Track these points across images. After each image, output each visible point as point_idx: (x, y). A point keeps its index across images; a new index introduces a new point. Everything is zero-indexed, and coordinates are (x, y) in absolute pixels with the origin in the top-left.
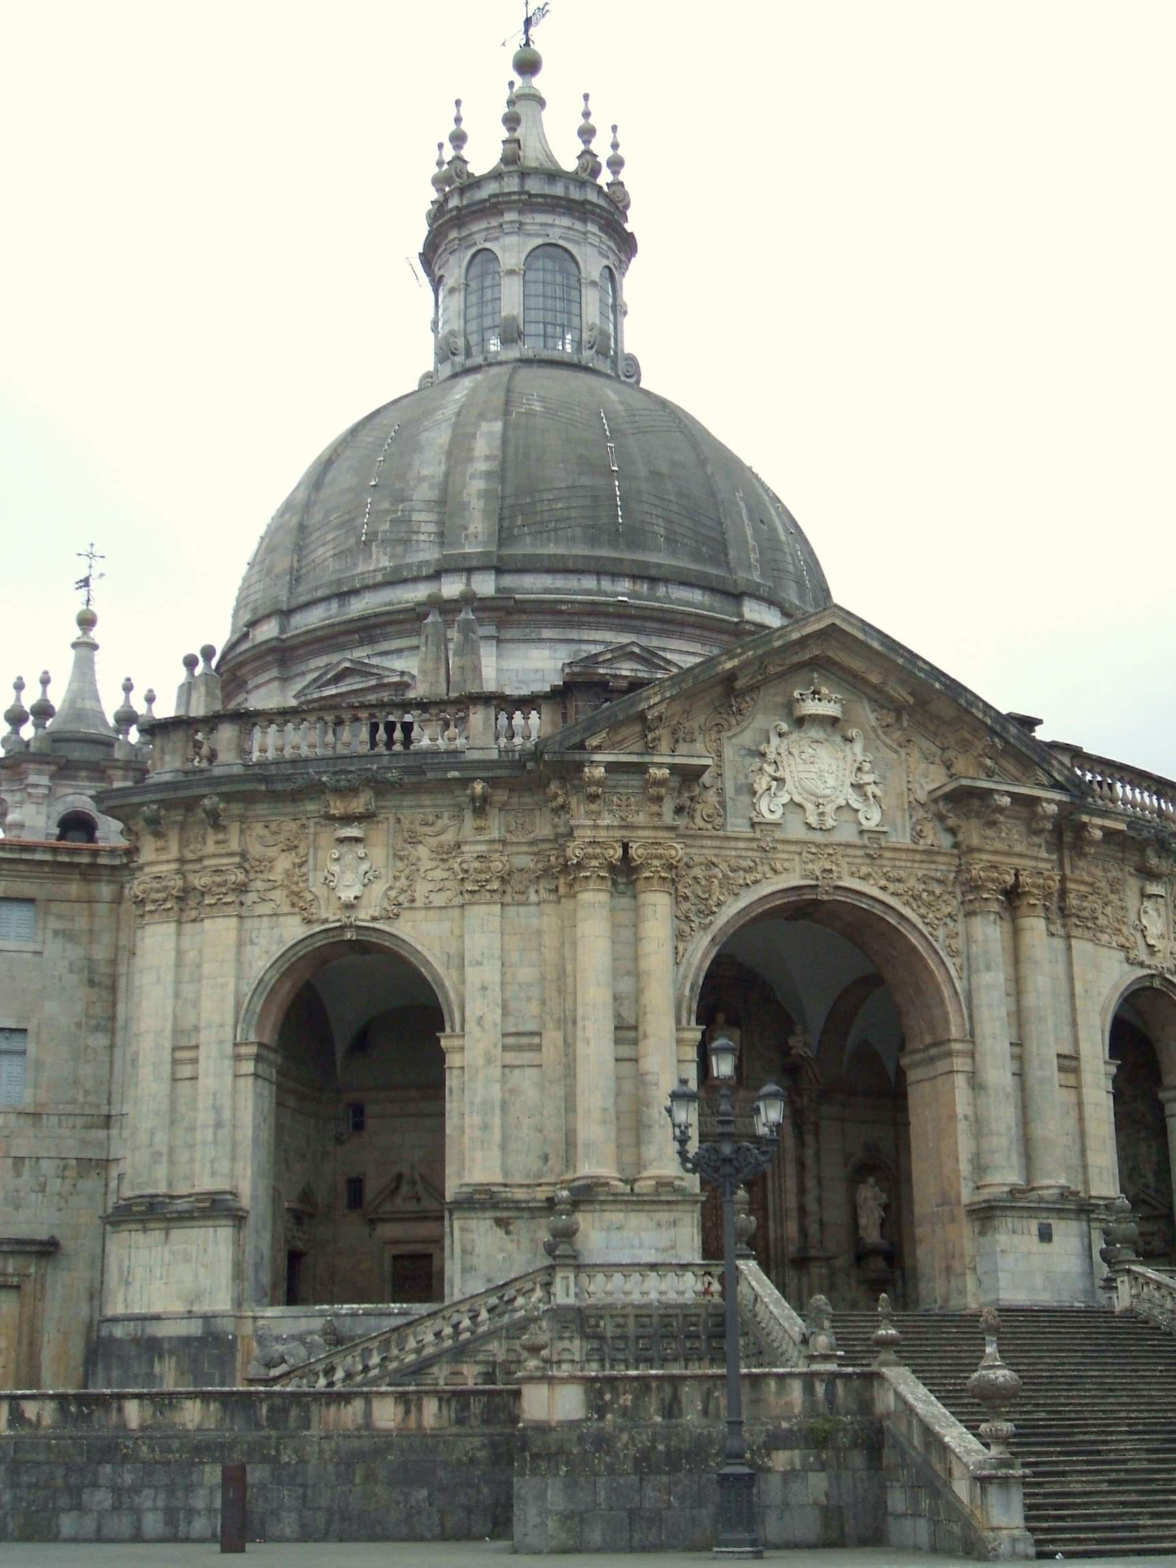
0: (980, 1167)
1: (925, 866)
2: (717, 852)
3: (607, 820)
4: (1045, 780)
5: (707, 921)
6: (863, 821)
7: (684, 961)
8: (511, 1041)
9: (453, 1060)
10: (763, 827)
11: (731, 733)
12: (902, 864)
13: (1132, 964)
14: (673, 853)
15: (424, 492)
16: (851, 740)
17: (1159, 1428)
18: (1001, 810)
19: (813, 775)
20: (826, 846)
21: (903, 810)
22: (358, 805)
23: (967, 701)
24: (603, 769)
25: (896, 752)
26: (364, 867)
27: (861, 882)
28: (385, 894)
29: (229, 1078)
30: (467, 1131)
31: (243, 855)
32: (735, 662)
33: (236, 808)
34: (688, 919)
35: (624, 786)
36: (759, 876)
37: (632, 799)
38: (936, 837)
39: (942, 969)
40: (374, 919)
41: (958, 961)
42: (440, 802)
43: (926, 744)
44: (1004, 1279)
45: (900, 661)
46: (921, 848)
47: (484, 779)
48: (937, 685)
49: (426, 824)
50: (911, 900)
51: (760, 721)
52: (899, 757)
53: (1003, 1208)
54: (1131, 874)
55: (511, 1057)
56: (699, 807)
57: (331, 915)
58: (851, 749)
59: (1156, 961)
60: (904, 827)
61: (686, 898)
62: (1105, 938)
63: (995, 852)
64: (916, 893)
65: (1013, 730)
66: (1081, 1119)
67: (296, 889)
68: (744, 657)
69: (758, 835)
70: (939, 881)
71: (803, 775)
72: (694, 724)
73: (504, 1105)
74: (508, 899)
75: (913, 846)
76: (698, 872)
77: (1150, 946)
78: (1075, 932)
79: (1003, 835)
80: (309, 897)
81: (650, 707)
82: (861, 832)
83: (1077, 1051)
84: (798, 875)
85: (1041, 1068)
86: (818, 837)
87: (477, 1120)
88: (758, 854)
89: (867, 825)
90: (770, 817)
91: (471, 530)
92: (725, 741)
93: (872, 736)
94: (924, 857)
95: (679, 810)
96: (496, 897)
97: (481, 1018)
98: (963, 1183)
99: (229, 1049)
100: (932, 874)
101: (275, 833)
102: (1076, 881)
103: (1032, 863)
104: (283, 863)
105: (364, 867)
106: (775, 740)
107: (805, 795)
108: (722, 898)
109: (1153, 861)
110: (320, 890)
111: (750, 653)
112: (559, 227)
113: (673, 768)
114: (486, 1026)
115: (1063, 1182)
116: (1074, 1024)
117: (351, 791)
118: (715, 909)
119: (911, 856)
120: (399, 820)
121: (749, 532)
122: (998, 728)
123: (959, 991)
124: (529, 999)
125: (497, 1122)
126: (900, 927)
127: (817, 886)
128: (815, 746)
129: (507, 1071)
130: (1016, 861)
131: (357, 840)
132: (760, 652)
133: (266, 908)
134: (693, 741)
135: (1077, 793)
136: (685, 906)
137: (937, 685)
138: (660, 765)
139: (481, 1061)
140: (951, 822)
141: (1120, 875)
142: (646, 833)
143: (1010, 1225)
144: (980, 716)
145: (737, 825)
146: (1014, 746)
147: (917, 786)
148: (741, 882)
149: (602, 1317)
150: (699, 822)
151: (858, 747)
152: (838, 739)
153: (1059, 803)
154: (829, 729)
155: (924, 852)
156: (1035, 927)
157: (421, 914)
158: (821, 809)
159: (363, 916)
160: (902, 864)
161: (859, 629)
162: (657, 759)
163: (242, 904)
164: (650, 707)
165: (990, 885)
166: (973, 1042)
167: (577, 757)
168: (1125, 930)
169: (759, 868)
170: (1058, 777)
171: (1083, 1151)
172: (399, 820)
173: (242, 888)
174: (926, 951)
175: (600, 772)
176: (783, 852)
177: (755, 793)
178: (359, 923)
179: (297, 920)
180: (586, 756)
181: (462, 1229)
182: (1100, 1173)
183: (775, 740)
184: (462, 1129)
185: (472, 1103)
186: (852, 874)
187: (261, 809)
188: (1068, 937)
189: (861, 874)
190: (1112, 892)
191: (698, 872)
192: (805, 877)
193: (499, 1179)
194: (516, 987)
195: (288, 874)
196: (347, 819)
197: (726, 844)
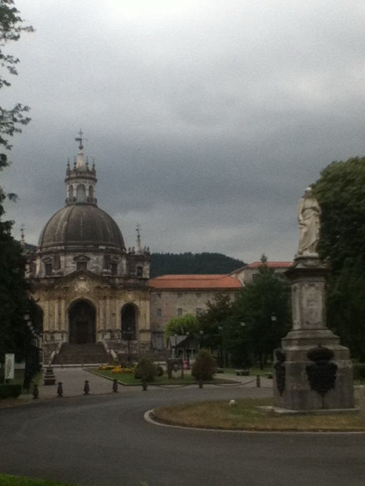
112: (81, 181)
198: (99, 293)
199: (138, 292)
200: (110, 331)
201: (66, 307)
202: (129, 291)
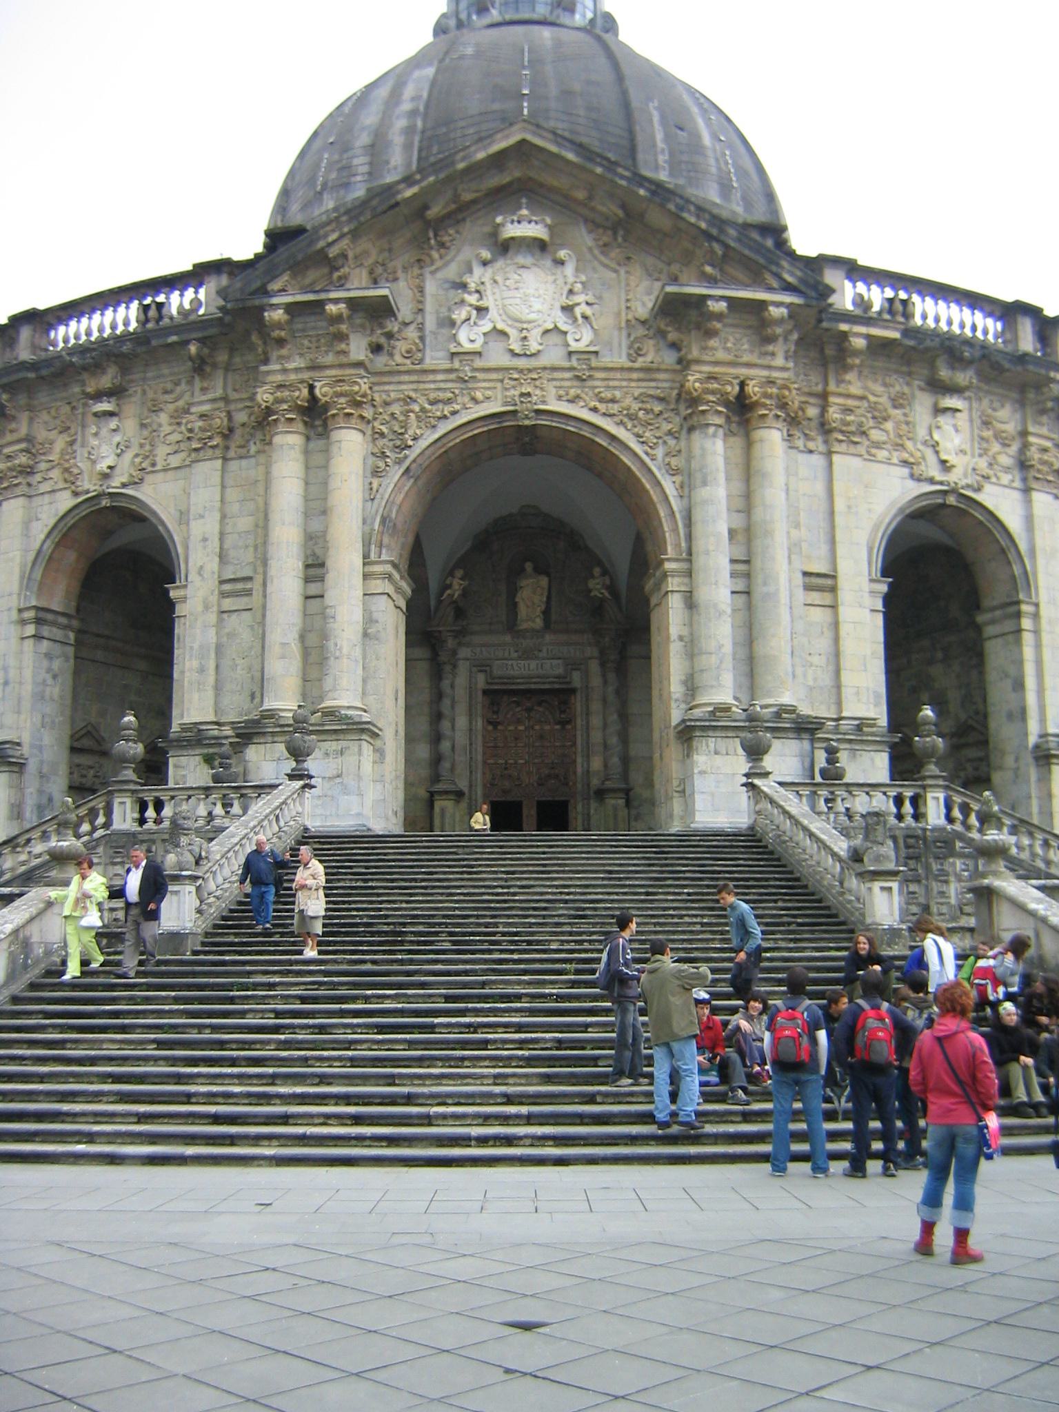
0: (692, 687)
1: (641, 384)
2: (414, 386)
3: (298, 362)
4: (775, 284)
5: (401, 456)
6: (572, 343)
7: (378, 496)
8: (227, 587)
9: (180, 610)
10: (462, 357)
11: (433, 268)
12: (616, 383)
13: (919, 480)
14: (356, 388)
15: (364, 139)
16: (562, 263)
17: (395, 967)
18: (719, 316)
19: (518, 301)
20: (530, 371)
21: (620, 329)
22: (106, 381)
23: (677, 206)
24: (281, 311)
25: (616, 271)
26: (117, 439)
27: (570, 405)
28: (133, 463)
29: (14, 641)
30: (187, 674)
31: (29, 439)
32: (415, 189)
33: (22, 399)
34: (384, 455)
35: (314, 328)
36: (457, 407)
37: (323, 340)
38: (652, 354)
39: (658, 489)
40: (124, 485)
41: (678, 479)
42: (176, 370)
43: (650, 261)
44: (700, 802)
45: (599, 170)
46: (637, 365)
47: (198, 340)
48: (642, 192)
49: (166, 392)
50: (625, 420)
51: (467, 253)
52: (619, 275)
53: (703, 728)
54: (921, 389)
55: (228, 604)
56: (397, 343)
57: (90, 485)
58: (562, 272)
59: (954, 477)
60: (620, 345)
61: (382, 435)
62: (882, 454)
63: (717, 363)
64: (632, 411)
65: (732, 232)
66: (836, 639)
67: (67, 465)
68: (424, 184)
69: (457, 365)
70: (661, 400)
71: (507, 302)
72: (398, 263)
73: (219, 649)
74: (231, 454)
75: (630, 364)
76: (396, 409)
77: (944, 462)
78: (837, 447)
79: (729, 345)
80: (76, 471)
81: (330, 245)
82: (570, 353)
83: (835, 570)
84: (500, 403)
85: (765, 584)
86: (522, 363)
87: (195, 664)
88: (458, 385)
89: (574, 346)
90: (467, 346)
91: (393, 163)
92: (428, 276)
93: (588, 256)
94: (641, 375)
95: (376, 349)
96: (218, 452)
97: (201, 567)
98: (673, 705)
99: (14, 615)
100: (651, 392)
101: (55, 418)
102: (840, 395)
103: (765, 373)
104: (60, 443)
105: (117, 439)
106: (478, 270)
107: (510, 323)
108: (418, 432)
109: (944, 373)
110: (83, 465)
111: (432, 179)
113: (352, 303)
114: (205, 576)
115: (786, 699)
116: (832, 542)
117: (96, 368)
118: (410, 443)
119: (626, 375)
120: (144, 392)
121: (659, 136)
122: (714, 232)
123: (675, 508)
124: (247, 547)
125: (212, 665)
126: (610, 448)
127: (515, 412)
128: (521, 271)
129: (225, 616)
130: (744, 372)
131: (111, 414)
132: (442, 176)
133: (45, 487)
134: (396, 279)
135: (813, 294)
136: (381, 442)
137: (642, 192)
138: (336, 301)
139: (200, 608)
140: (673, 336)
141: (906, 390)
142: (333, 372)
143: (712, 745)
144: (693, 220)
145: (434, 358)
146: (733, 249)
147: (638, 304)
148: (439, 414)
149: (153, 842)
150: (398, 359)
151: (569, 269)
152: (548, 263)
153: (789, 306)
154: (538, 253)
155: (641, 370)
156: (772, 439)
157: (160, 476)
158: (525, 333)
159: (115, 485)
160: (616, 383)
161: (550, 141)
162: (333, 295)
163: (29, 485)
164: (330, 245)
165: (712, 398)
166: (690, 561)
167: (257, 302)
168: (909, 444)
169: (459, 399)
170: (790, 279)
171: (837, 672)
172: (144, 392)
173: (28, 471)
174: (639, 470)
175: (278, 315)
176: (485, 381)
177: (452, 324)
178: (111, 490)
179: (67, 494)
180: (265, 301)
181: (176, 766)
182: (857, 693)
183: (478, 270)
184: (183, 672)
185: (191, 648)
186: (560, 398)
187: (42, 397)
188: (829, 454)
189: (569, 397)
190: (895, 407)
191: (396, 409)
192: (506, 404)
193: (211, 717)
194: (236, 536)
195: (63, 453)
196: (98, 396)
197: (424, 378)
198: (684, 364)
199: (1007, 418)
200: (806, 728)
201: (371, 495)
202: (938, 387)
